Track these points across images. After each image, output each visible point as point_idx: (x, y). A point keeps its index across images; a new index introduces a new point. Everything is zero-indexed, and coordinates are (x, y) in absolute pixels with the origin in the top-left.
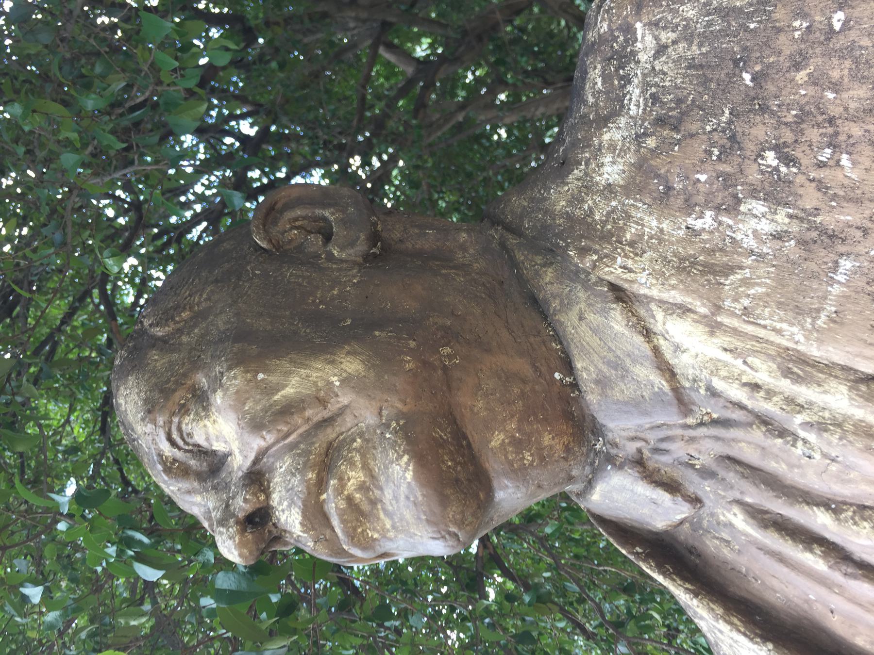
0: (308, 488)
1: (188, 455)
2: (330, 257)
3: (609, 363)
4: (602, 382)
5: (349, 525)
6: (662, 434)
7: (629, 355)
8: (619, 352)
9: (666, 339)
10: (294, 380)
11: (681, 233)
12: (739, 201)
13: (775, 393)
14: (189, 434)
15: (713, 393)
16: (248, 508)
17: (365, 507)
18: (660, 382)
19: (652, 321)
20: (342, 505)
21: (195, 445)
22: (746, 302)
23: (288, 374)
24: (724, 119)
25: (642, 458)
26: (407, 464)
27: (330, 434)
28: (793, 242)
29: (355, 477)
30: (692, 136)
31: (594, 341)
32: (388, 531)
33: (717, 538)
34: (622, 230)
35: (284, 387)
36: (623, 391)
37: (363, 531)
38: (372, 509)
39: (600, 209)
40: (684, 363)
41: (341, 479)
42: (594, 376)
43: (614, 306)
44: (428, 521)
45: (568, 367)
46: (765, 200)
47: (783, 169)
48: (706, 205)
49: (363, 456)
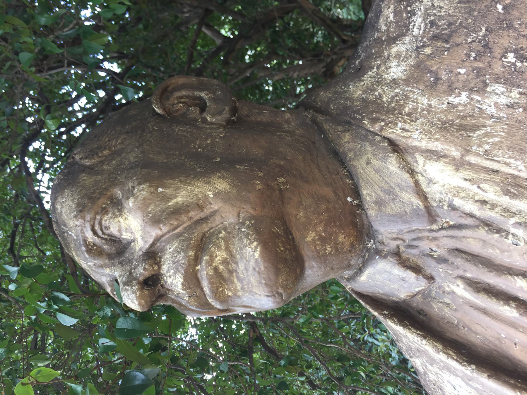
0: (189, 261)
1: (104, 241)
2: (205, 121)
3: (385, 191)
4: (379, 203)
5: (215, 285)
6: (414, 236)
7: (398, 186)
8: (392, 184)
9: (423, 176)
10: (183, 193)
11: (444, 107)
12: (486, 85)
13: (497, 206)
14: (106, 227)
15: (453, 208)
16: (147, 274)
17: (226, 275)
18: (417, 203)
19: (415, 164)
20: (211, 272)
21: (109, 235)
22: (487, 147)
23: (178, 189)
24: (481, 34)
25: (399, 252)
26: (256, 247)
27: (205, 228)
28: (521, 110)
29: (220, 255)
30: (457, 45)
31: (376, 177)
32: (238, 291)
33: (441, 302)
34: (403, 106)
35: (175, 197)
36: (392, 208)
37: (223, 290)
38: (230, 276)
39: (387, 95)
40: (434, 192)
41: (211, 256)
42: (374, 199)
43: (392, 155)
44: (266, 284)
45: (357, 193)
46: (504, 84)
47: (519, 64)
48: (463, 89)
49: (226, 242)
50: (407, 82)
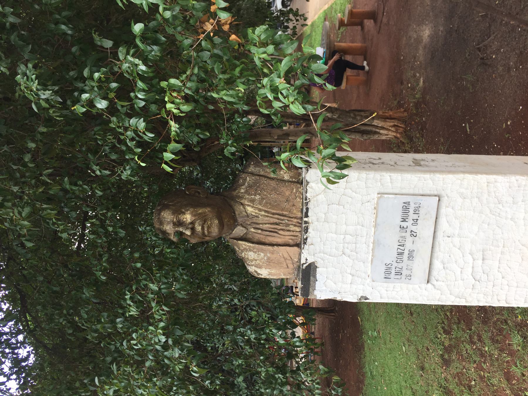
4: (239, 214)
29: (209, 223)
40: (249, 212)
45: (234, 213)
50: (244, 193)
